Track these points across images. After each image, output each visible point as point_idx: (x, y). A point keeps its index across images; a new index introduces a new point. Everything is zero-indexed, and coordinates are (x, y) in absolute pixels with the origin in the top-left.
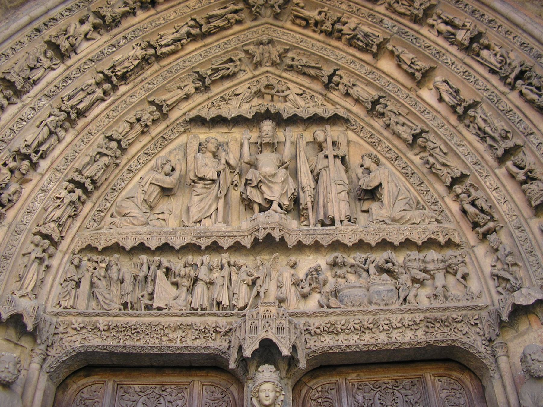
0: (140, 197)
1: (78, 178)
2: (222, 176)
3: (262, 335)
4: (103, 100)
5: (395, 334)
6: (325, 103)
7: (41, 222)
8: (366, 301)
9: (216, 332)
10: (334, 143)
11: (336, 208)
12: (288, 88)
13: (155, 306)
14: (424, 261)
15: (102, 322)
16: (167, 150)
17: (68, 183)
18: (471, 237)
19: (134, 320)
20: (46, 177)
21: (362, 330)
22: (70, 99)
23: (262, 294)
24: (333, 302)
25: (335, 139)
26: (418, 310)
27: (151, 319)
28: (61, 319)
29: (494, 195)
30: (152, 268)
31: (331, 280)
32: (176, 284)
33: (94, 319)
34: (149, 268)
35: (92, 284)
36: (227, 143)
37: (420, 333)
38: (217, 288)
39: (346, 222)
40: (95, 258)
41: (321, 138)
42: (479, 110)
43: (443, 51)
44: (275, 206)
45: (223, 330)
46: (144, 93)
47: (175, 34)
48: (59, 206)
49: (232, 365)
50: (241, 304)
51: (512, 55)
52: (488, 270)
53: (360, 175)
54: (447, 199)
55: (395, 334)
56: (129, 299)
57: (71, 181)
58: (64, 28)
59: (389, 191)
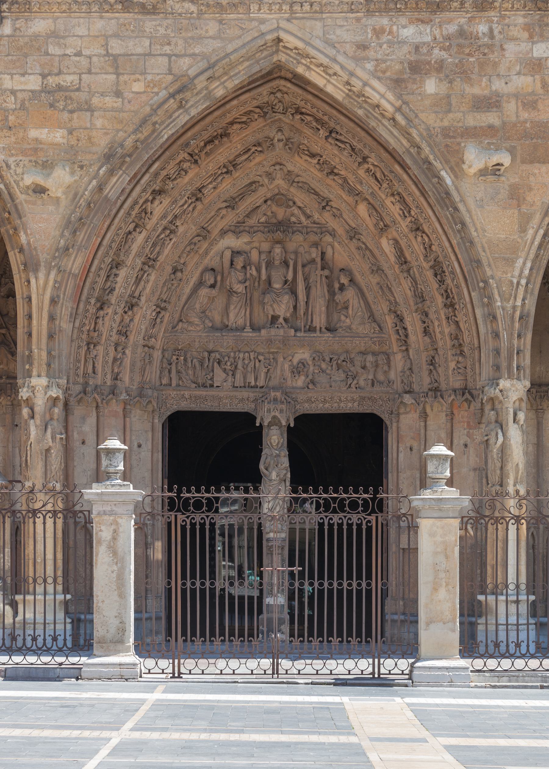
0: (197, 306)
1: (163, 305)
2: (248, 290)
3: (273, 414)
4: (168, 244)
5: (342, 405)
6: (320, 217)
7: (146, 338)
8: (328, 386)
9: (248, 400)
10: (323, 254)
11: (318, 321)
12: (294, 203)
13: (215, 385)
14: (365, 361)
15: (187, 394)
16: (208, 257)
17: (155, 307)
18: (395, 348)
19: (204, 393)
20: (144, 308)
21: (325, 401)
22: (151, 254)
23: (272, 379)
24: (311, 386)
25: (324, 251)
26: (356, 393)
27: (214, 393)
28: (164, 392)
29: (409, 328)
30: (211, 360)
31: (311, 368)
32: (225, 370)
33: (182, 393)
34: (209, 360)
35: (178, 372)
36: (250, 252)
37: (356, 404)
38: (249, 374)
39: (323, 329)
40: (177, 353)
41: (314, 255)
42: (411, 272)
43: (397, 222)
44: (281, 320)
45: (252, 399)
46: (193, 227)
47: (214, 183)
48: (154, 325)
49: (258, 425)
50: (261, 385)
51: (433, 248)
52: (400, 369)
53: (337, 290)
54: (387, 316)
55: (342, 405)
56: (200, 381)
57: (158, 306)
58: (144, 207)
59: (353, 307)
